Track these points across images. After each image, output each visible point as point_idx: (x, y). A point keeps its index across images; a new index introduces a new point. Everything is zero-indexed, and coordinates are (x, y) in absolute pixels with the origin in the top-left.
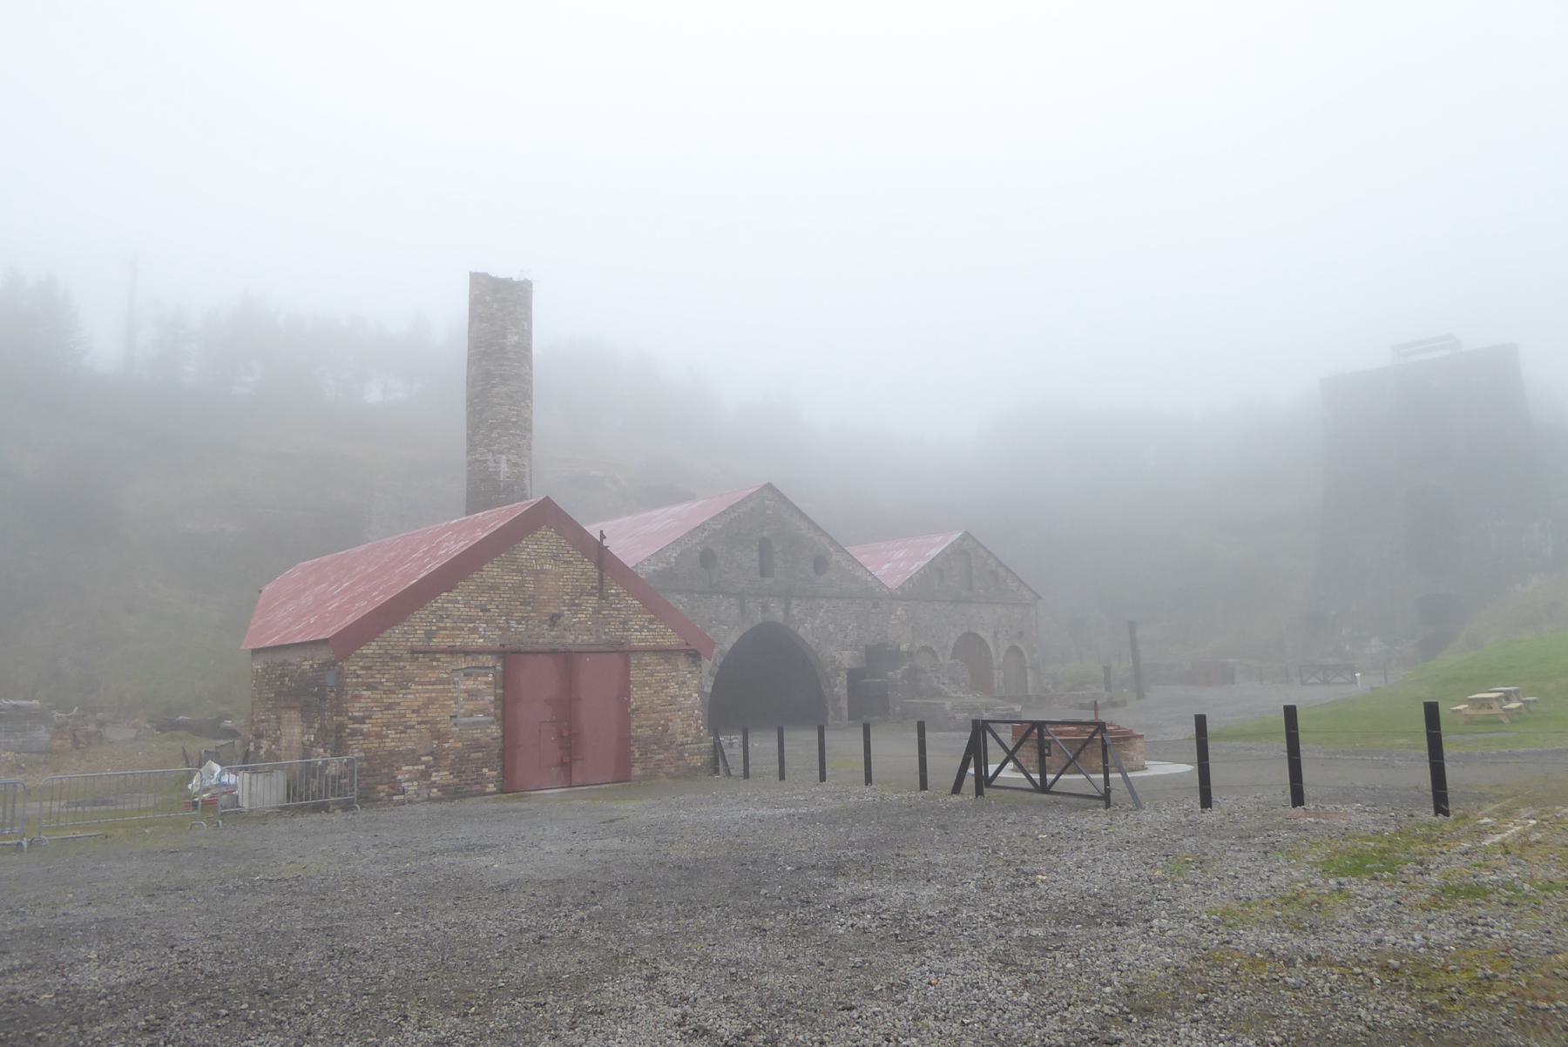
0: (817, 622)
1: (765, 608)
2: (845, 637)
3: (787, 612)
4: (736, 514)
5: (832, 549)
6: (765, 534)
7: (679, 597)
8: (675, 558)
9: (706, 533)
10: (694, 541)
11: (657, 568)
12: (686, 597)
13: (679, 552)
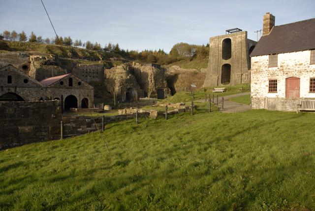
1: (9, 90)
3: (15, 90)
6: (10, 75)
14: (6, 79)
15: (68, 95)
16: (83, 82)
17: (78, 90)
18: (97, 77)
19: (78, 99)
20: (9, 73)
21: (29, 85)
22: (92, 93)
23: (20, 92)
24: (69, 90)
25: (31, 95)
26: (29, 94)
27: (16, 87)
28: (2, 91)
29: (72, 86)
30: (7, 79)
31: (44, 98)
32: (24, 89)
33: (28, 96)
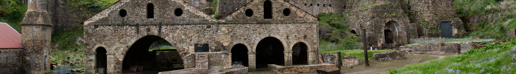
0: (176, 34)
1: (149, 30)
2: (191, 40)
3: (160, 31)
5: (185, 5)
7: (109, 27)
8: (108, 14)
9: (122, 4)
10: (117, 7)
11: (100, 18)
12: (112, 27)
13: (110, 12)
15: (263, 37)
16: (293, 9)
17: (284, 26)
18: (330, 6)
19: (285, 44)
21: (184, 19)
22: (315, 31)
23: (168, 35)
24: (264, 26)
25: (188, 40)
26: (183, 37)
27: (160, 25)
28: (138, 32)
29: (271, 17)
30: (145, 10)
31: (212, 45)
32: (174, 27)
33: (182, 41)
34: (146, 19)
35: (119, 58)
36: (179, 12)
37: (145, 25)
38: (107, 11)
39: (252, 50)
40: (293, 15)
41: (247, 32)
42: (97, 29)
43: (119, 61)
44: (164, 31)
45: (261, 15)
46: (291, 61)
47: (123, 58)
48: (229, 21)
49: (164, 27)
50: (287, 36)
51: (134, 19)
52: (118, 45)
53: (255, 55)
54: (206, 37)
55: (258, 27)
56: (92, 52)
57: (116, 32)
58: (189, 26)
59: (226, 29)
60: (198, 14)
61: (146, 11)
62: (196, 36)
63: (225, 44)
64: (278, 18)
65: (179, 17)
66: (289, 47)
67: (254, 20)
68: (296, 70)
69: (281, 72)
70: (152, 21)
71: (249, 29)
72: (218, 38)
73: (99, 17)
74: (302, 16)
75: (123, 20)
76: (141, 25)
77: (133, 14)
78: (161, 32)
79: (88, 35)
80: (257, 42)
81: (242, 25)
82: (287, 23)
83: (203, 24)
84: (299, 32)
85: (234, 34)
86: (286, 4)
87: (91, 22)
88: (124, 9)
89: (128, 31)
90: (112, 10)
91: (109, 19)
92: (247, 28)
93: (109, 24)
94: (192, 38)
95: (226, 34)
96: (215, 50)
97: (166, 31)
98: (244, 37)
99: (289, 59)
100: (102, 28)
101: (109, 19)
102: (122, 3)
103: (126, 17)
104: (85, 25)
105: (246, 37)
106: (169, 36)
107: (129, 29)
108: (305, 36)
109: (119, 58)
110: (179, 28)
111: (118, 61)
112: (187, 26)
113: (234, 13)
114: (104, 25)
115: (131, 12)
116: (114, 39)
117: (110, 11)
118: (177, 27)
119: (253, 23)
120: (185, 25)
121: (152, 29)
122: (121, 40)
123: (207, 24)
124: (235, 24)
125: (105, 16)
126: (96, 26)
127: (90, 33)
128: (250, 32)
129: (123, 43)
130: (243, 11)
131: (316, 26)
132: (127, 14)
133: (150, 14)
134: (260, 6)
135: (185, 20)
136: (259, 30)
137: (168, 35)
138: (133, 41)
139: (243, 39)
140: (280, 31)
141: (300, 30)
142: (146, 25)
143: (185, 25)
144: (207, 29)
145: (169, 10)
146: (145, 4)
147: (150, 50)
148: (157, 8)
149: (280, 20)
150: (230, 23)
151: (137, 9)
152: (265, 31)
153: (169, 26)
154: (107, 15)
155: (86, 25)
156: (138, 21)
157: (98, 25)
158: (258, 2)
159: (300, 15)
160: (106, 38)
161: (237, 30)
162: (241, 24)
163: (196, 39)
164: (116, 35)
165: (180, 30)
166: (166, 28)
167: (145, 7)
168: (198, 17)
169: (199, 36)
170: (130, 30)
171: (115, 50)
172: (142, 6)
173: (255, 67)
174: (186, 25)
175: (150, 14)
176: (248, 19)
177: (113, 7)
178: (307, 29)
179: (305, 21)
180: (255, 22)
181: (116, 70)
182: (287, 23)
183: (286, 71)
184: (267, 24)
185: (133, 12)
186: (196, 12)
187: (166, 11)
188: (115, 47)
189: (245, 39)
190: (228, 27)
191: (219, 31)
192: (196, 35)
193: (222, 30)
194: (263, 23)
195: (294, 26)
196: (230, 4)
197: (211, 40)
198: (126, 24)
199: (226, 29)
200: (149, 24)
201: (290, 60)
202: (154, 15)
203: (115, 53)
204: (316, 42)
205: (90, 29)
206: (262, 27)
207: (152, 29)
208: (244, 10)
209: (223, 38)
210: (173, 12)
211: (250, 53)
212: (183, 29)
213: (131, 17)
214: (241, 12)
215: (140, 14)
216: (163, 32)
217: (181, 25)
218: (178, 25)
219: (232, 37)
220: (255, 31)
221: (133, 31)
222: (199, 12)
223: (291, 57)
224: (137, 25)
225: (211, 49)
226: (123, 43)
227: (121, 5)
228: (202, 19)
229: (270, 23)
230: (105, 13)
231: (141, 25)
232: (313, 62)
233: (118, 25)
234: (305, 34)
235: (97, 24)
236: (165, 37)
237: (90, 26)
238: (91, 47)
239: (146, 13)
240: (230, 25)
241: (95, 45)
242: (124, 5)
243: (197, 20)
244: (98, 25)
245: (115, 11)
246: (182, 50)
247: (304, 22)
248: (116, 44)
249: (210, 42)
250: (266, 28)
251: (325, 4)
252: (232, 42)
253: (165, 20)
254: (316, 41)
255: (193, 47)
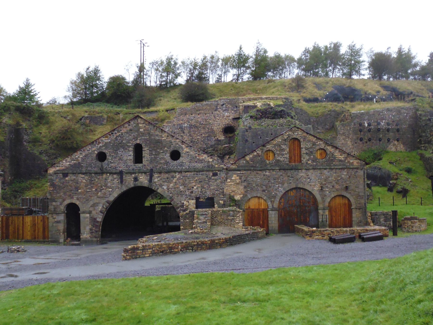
0: (172, 185)
1: (136, 179)
2: (192, 192)
3: (150, 180)
4: (120, 133)
6: (138, 142)
7: (83, 176)
8: (81, 158)
9: (101, 145)
10: (93, 149)
11: (71, 163)
13: (84, 155)
14: (130, 155)
19: (318, 197)
20: (136, 138)
23: (161, 186)
24: (289, 173)
27: (151, 173)
30: (131, 153)
34: (132, 164)
35: (97, 218)
36: (175, 155)
37: (131, 173)
38: (81, 154)
39: (273, 206)
40: (330, 157)
41: (265, 181)
42: (67, 179)
43: (98, 222)
44: (156, 180)
45: (286, 157)
46: (327, 221)
47: (102, 217)
48: (242, 166)
49: (157, 175)
50: (322, 187)
51: (116, 164)
52: (95, 200)
53: (277, 212)
54: (212, 188)
55: (281, 175)
56: (59, 210)
57: (93, 182)
58: (188, 174)
59: (238, 178)
60: (201, 158)
61: (132, 154)
62: (199, 187)
63: (237, 197)
64: (309, 162)
65: (175, 161)
66: (324, 202)
67: (276, 165)
68: (330, 234)
69: (309, 237)
70: (140, 167)
71: (269, 177)
72: (227, 190)
73: (69, 162)
74: (342, 159)
75: (102, 166)
76: (127, 173)
77: (115, 158)
78: (153, 181)
79: (53, 187)
80: (280, 195)
81: (259, 172)
82: (320, 169)
83: (208, 171)
84: (338, 181)
85: (249, 184)
86: (320, 143)
87: (58, 168)
88: (103, 151)
89: (108, 180)
90: (87, 152)
91: (82, 164)
92: (266, 175)
93: (82, 172)
94: (194, 189)
95: (238, 184)
96: (224, 204)
97: (159, 180)
98: (262, 187)
99: (324, 218)
100: (73, 177)
101: (82, 164)
102: (100, 143)
103: (106, 162)
104: (50, 174)
105: (264, 188)
106: (163, 187)
107: (111, 178)
108: (346, 187)
109: (97, 218)
110: (175, 177)
111: (95, 222)
112: (187, 173)
113: (248, 156)
114: (76, 173)
115: (113, 156)
116: (90, 192)
117: (84, 154)
118: (173, 176)
119: (274, 170)
120: (184, 173)
121: (141, 177)
122: (99, 193)
123: (213, 171)
124: (250, 170)
125: (77, 161)
126: (65, 175)
127: (57, 184)
128: (270, 181)
129: (102, 197)
130: (260, 152)
131: (363, 173)
132: (108, 157)
133: (138, 158)
134: (283, 147)
135: (184, 166)
136: (283, 179)
137: (162, 186)
138: (115, 195)
139: (260, 190)
140: (311, 179)
141: (339, 178)
142: (133, 173)
143: (184, 172)
144: (213, 178)
145: (162, 153)
146: (131, 144)
147: (147, 204)
148: (147, 149)
149: (311, 165)
150: (244, 169)
151: (120, 152)
152: (290, 180)
153: (162, 174)
154: (80, 159)
155: (51, 173)
156: (122, 167)
157: (68, 173)
158: (280, 141)
159: (340, 157)
160: (79, 191)
161: (252, 178)
162: (257, 170)
163: (198, 191)
164: (92, 187)
165: (176, 179)
166: (159, 177)
167: (131, 149)
168: (201, 161)
169: (203, 187)
170: (111, 180)
171: (91, 206)
172: (127, 147)
173: (277, 228)
174: (186, 172)
175: (138, 158)
176: (267, 164)
177: (88, 148)
178: (350, 177)
179: (346, 166)
180: (277, 168)
181: (93, 234)
182: (320, 169)
183: (317, 236)
184: (294, 170)
185: (115, 156)
186: (199, 155)
187: (159, 153)
188: (91, 203)
189: (264, 191)
190: (241, 175)
191: (229, 180)
192: (199, 186)
193: (232, 179)
194: (287, 170)
195: (332, 172)
196: (254, 141)
197: (219, 192)
198: (106, 172)
199: (238, 178)
200: (137, 171)
201: (326, 219)
202: (143, 159)
203: (91, 211)
204: (363, 196)
205: (56, 178)
206: (287, 174)
207: (141, 177)
208: (262, 152)
209: (234, 189)
210: (168, 155)
211: (270, 210)
212: (182, 177)
213: (112, 161)
214: (257, 154)
215: (125, 158)
216: (155, 182)
217: (179, 172)
218: (175, 172)
219: (245, 187)
220: (277, 179)
221: (116, 181)
222: (202, 155)
223: (326, 215)
224: (121, 174)
225: (219, 204)
226: (102, 197)
227: (99, 146)
228: (206, 164)
229: (297, 169)
230: (77, 157)
231: (127, 173)
232: (358, 223)
233: (96, 173)
234: (347, 184)
235: (66, 172)
236: (158, 189)
237: (57, 174)
238: (59, 203)
239: (133, 157)
240: (243, 172)
241: (64, 200)
242: (103, 146)
243: (199, 166)
244: (68, 173)
245: (91, 153)
246: (180, 206)
247: (345, 167)
248: (92, 198)
249: (217, 195)
250: (293, 176)
251: (389, 137)
252: (246, 195)
253: (157, 166)
254: (363, 194)
255: (194, 201)
